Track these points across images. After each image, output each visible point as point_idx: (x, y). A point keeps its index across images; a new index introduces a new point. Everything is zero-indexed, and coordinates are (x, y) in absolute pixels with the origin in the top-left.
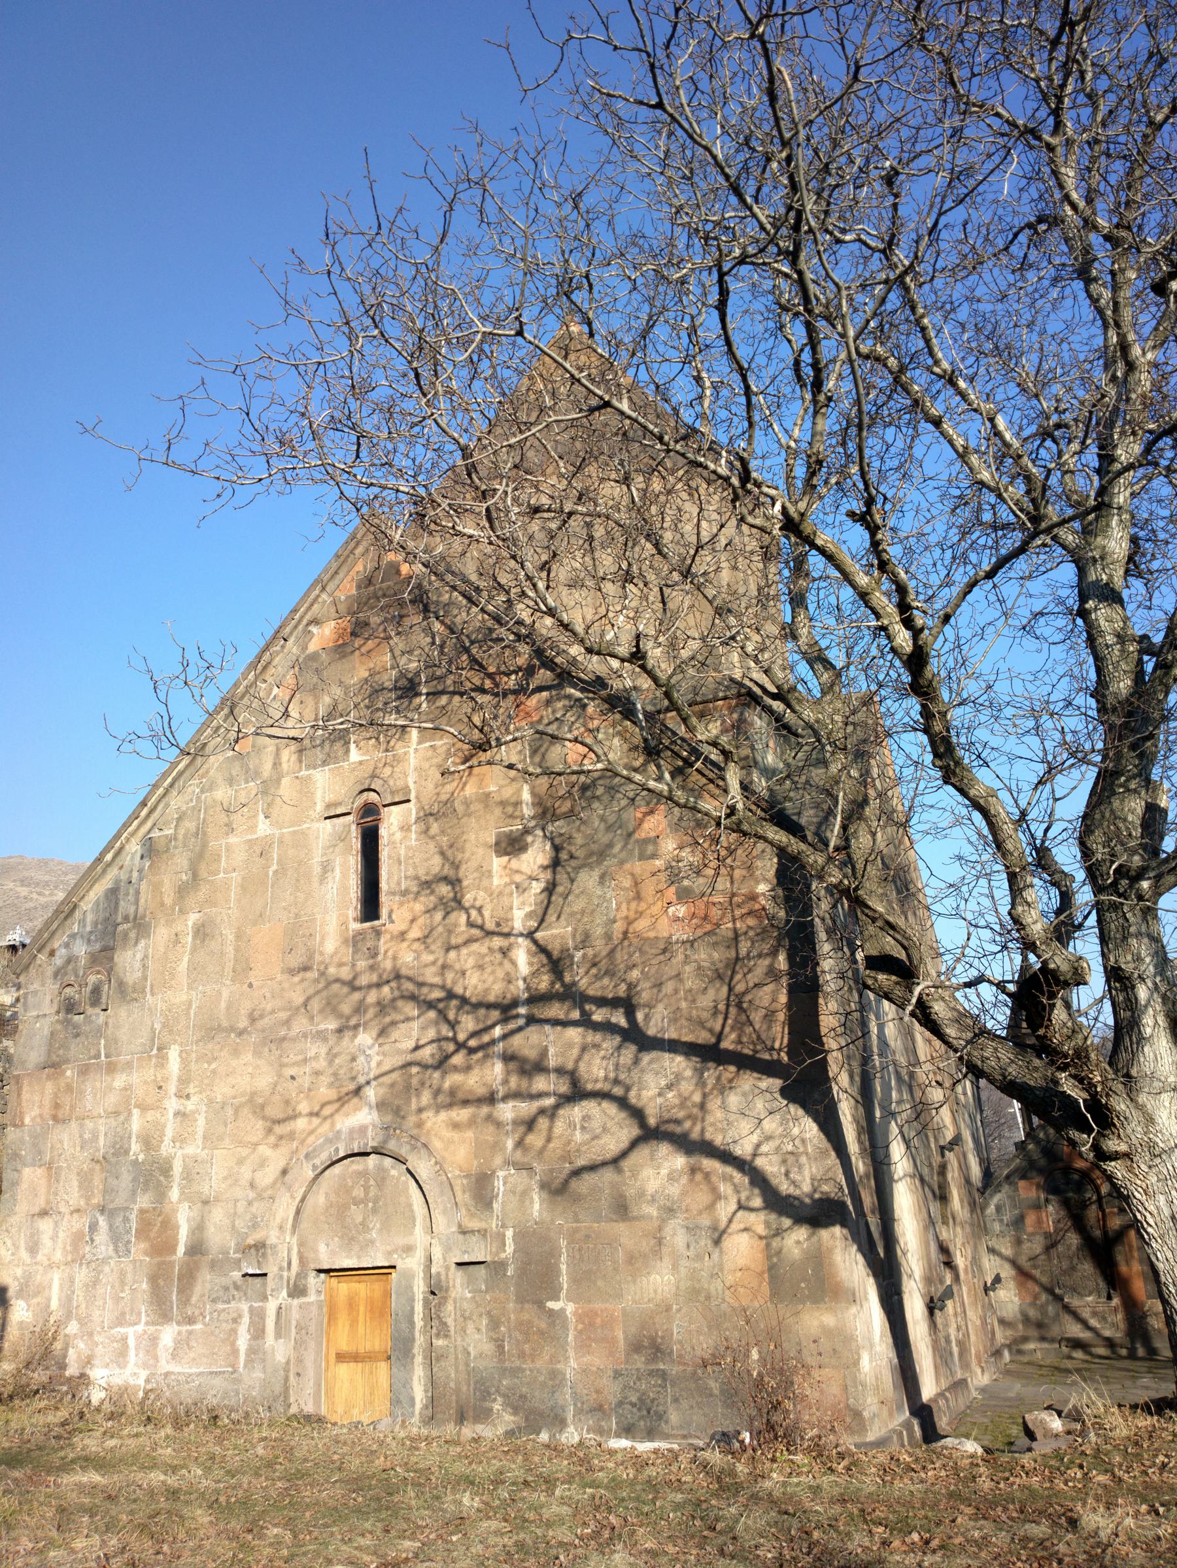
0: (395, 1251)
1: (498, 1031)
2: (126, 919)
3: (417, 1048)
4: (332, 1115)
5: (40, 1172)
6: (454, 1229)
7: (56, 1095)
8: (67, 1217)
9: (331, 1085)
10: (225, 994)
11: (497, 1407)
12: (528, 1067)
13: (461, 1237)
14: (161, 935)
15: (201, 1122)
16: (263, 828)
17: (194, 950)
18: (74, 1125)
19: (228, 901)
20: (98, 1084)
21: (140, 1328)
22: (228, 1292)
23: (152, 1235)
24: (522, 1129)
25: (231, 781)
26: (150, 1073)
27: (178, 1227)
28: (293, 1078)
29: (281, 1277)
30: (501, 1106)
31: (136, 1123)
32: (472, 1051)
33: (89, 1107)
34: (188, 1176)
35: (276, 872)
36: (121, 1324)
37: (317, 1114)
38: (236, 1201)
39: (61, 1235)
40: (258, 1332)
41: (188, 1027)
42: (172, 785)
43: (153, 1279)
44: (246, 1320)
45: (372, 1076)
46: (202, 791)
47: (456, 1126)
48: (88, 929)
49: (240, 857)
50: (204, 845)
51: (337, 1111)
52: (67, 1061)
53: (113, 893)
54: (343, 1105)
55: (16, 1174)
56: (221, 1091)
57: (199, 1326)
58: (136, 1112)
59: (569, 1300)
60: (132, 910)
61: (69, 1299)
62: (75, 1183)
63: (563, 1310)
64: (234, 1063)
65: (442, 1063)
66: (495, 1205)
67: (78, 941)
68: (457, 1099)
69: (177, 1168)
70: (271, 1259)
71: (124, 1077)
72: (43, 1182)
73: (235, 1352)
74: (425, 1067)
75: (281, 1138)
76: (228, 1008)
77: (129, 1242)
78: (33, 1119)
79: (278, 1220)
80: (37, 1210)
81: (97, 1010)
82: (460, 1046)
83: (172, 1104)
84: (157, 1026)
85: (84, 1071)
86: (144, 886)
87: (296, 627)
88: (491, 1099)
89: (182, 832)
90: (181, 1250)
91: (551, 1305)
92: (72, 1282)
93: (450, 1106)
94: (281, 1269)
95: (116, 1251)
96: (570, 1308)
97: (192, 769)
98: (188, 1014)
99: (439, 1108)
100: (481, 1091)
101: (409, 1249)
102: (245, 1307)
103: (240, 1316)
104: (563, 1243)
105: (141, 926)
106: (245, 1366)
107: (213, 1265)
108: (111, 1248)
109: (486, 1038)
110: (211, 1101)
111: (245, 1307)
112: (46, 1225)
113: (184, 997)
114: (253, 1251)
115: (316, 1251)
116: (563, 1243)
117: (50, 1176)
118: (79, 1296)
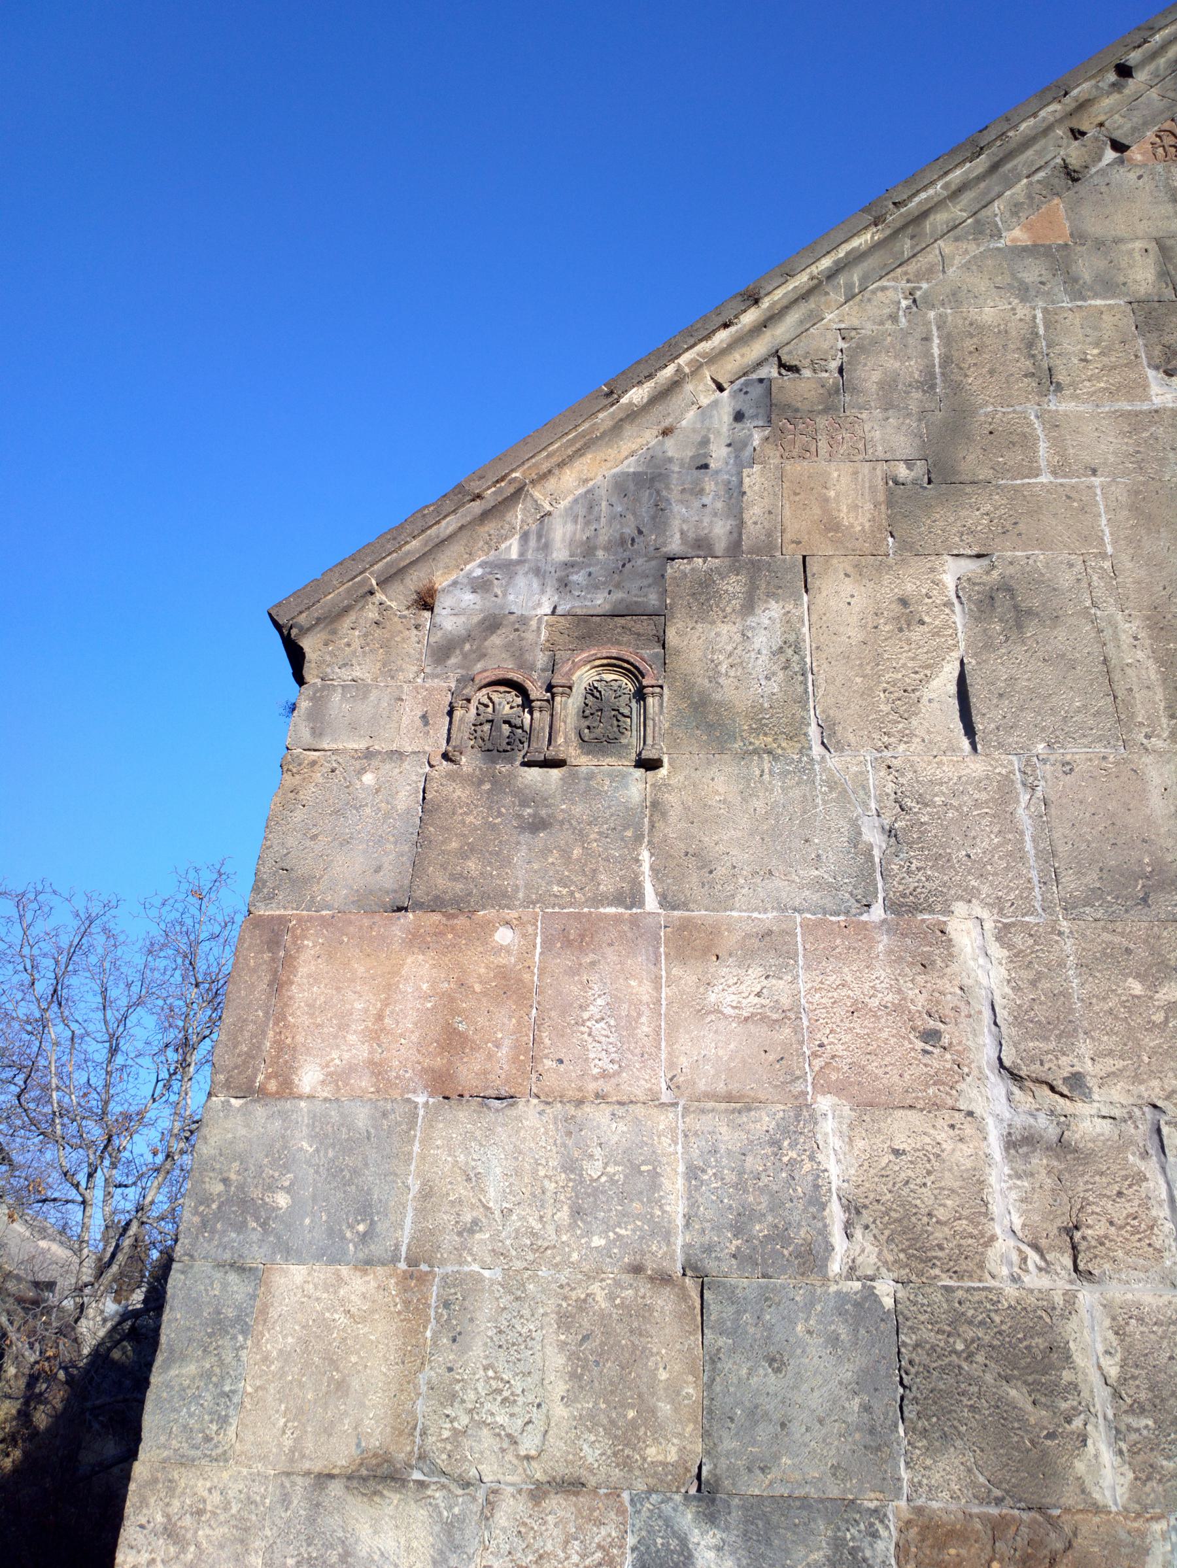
2: (702, 546)
7: (449, 1003)
8: (510, 1509)
20: (642, 990)
33: (599, 1061)
42: (832, 275)
52: (501, 898)
53: (647, 485)
58: (824, 1103)
60: (720, 530)
71: (753, 978)
78: (337, 1078)
80: (341, 1454)
85: (575, 938)
105: (765, 568)
117: (413, 1311)
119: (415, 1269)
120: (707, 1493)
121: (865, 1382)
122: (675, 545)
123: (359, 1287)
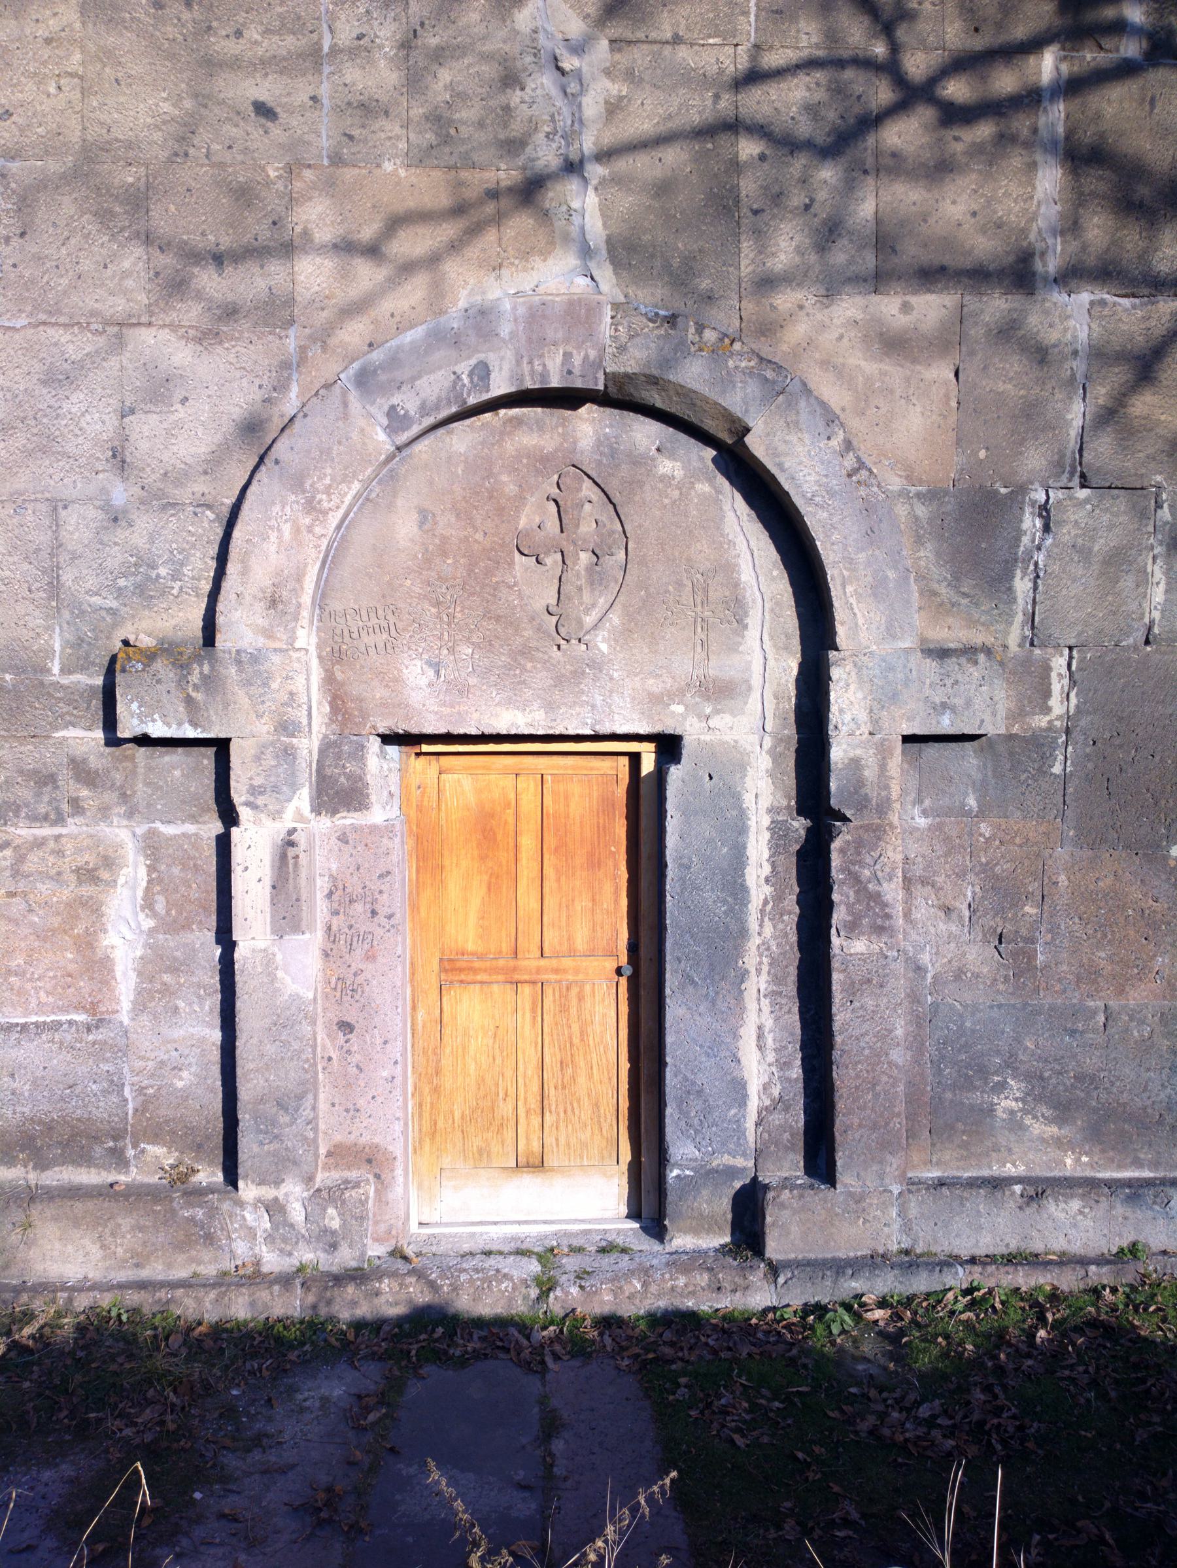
0: (676, 695)
1: (1048, 65)
3: (753, 77)
4: (433, 261)
9: (419, 158)
11: (1006, 1104)
12: (1143, 191)
24: (1119, 375)
28: (264, 111)
30: (1058, 297)
32: (954, 115)
37: (373, 251)
38: (57, 506)
45: (588, 143)
47: (894, 344)
51: (454, 247)
54: (474, 231)
65: (846, 138)
68: (892, 261)
70: (241, 696)
73: (98, 968)
74: (785, 143)
75: (230, 312)
82: (912, 95)
88: (1019, 274)
93: (878, 281)
99: (832, 287)
100: (984, 247)
102: (122, 834)
103: (109, 862)
106: (139, 1007)
109: (1005, 82)
115: (395, 682)
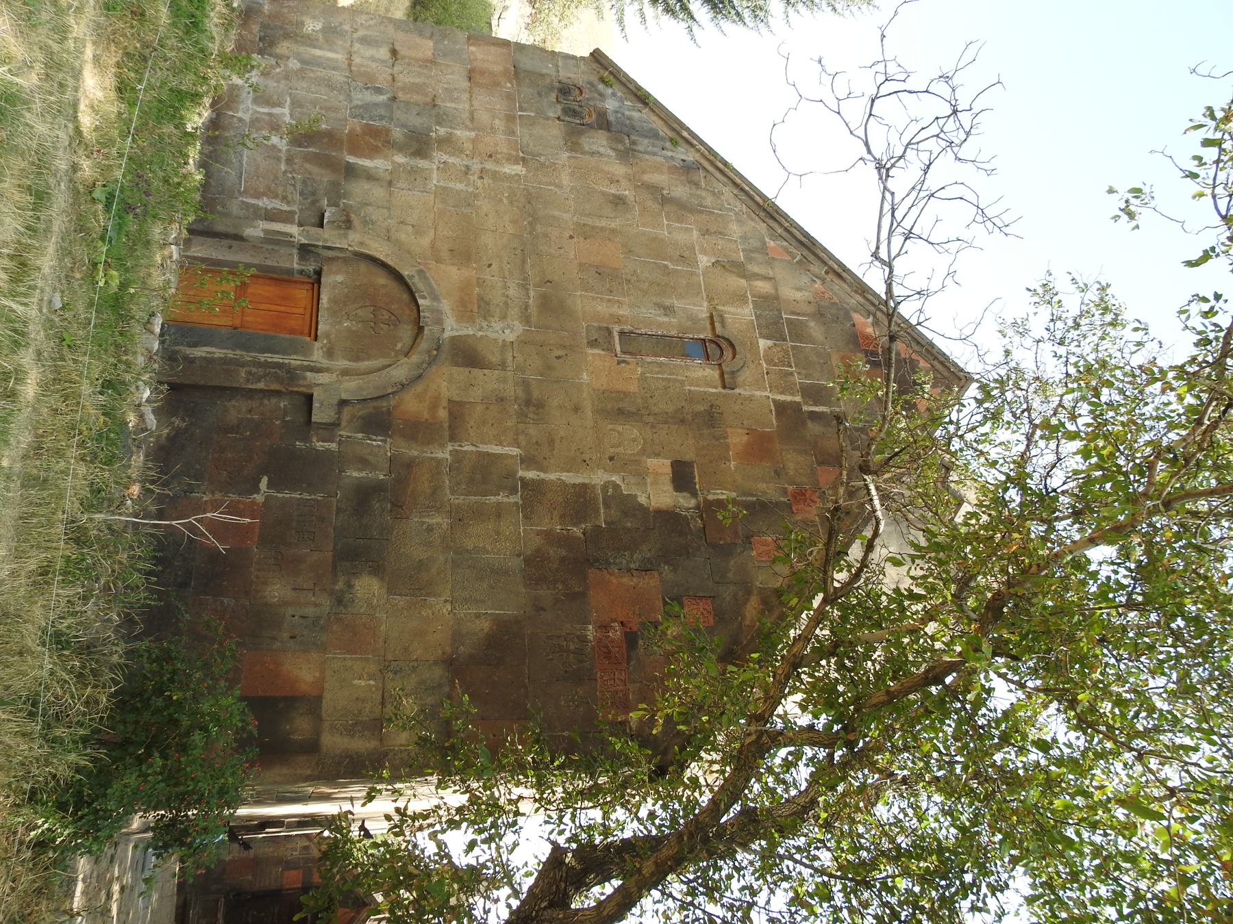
5: (429, 53)
6: (344, 396)
8: (390, 71)
10: (566, 216)
13: (336, 402)
14: (619, 169)
15: (460, 186)
16: (704, 261)
17: (604, 194)
18: (466, 84)
19: (644, 225)
21: (287, 119)
22: (310, 194)
23: (367, 138)
25: (744, 238)
26: (503, 148)
27: (371, 158)
28: (490, 265)
29: (318, 240)
31: (462, 134)
34: (413, 171)
35: (666, 267)
36: (292, 103)
39: (374, 65)
40: (271, 216)
41: (540, 183)
43: (329, 135)
44: (285, 208)
46: (736, 214)
48: (627, 113)
49: (681, 237)
50: (692, 211)
52: (519, 84)
55: (428, 35)
56: (485, 205)
57: (283, 167)
58: (473, 134)
59: (266, 498)
60: (641, 148)
61: (319, 65)
62: (417, 80)
63: (257, 490)
64: (507, 218)
66: (360, 435)
67: (617, 104)
69: (422, 163)
70: (336, 232)
71: (502, 128)
72: (421, 55)
73: (258, 196)
76: (554, 217)
77: (363, 118)
79: (368, 242)
80: (397, 48)
81: (559, 113)
83: (476, 166)
84: (542, 159)
85: (509, 97)
86: (659, 159)
87: (873, 304)
89: (704, 194)
90: (352, 159)
91: (265, 480)
92: (334, 69)
94: (326, 240)
95: (356, 107)
96: (259, 498)
97: (754, 207)
98: (550, 184)
101: (330, 353)
103: (288, 203)
104: (319, 497)
105: (627, 154)
106: (243, 202)
107: (335, 185)
108: (360, 103)
110: (476, 196)
111: (295, 208)
112: (384, 53)
113: (565, 183)
114: (344, 218)
115: (337, 273)
116: (319, 497)
117: (426, 61)
118: (321, 73)
119: (433, 62)
120: (394, 99)
121: (415, 127)
122: (633, 137)
123: (430, 54)
